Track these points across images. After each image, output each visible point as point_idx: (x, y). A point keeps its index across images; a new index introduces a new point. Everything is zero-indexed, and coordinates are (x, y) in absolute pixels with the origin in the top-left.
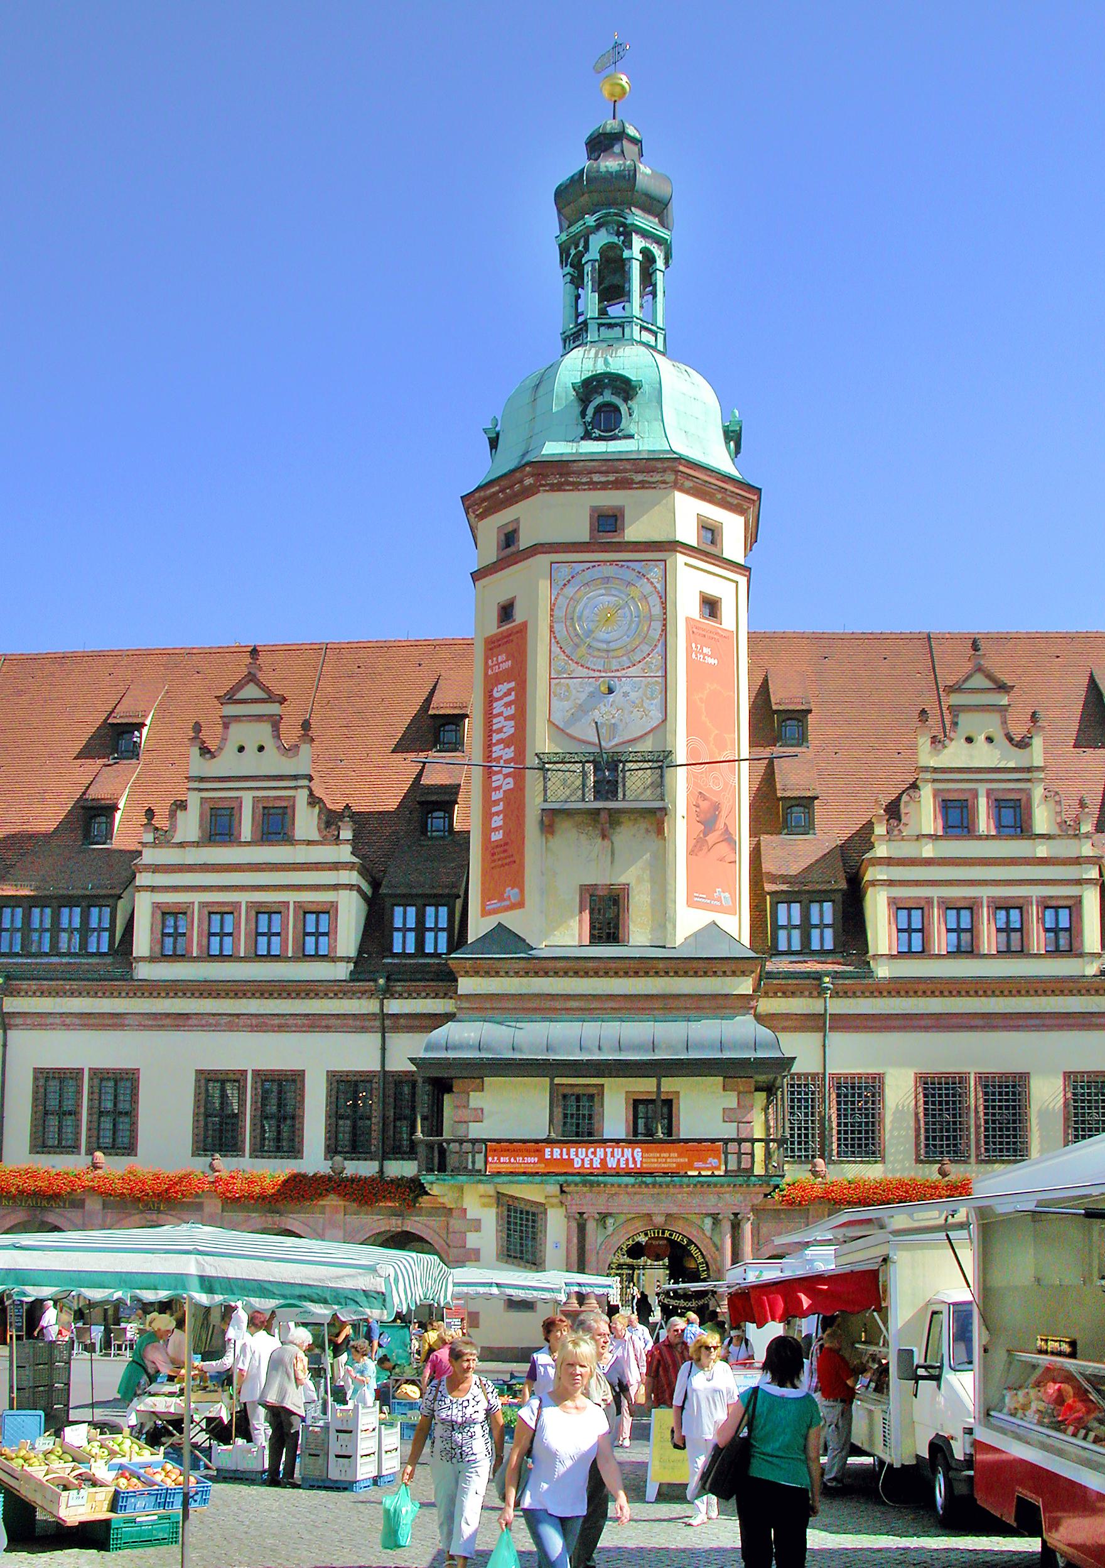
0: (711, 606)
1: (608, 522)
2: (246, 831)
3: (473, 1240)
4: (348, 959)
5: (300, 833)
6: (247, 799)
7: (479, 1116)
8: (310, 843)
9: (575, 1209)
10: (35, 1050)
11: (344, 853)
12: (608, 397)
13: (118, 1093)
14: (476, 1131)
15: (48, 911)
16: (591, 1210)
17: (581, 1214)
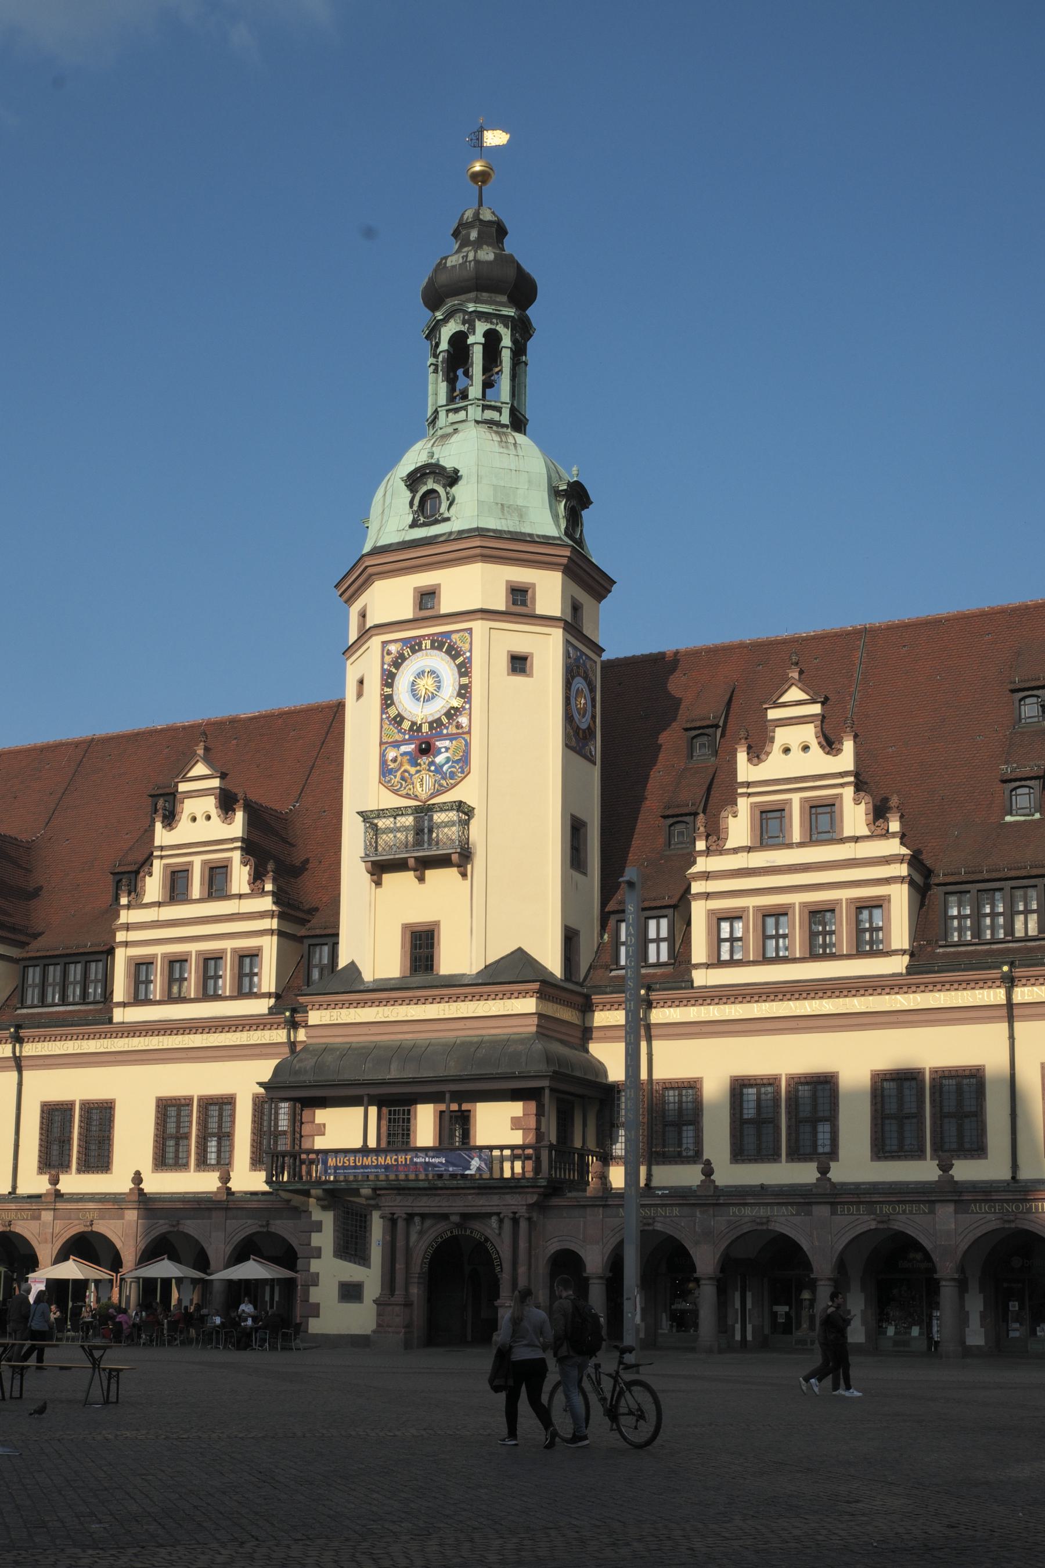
0: (519, 663)
1: (427, 597)
2: (196, 891)
3: (316, 1240)
4: (269, 995)
5: (235, 890)
6: (197, 861)
7: (321, 1130)
8: (240, 896)
9: (387, 1211)
10: (50, 1086)
11: (266, 903)
12: (430, 484)
13: (100, 1117)
14: (320, 1143)
15: (79, 966)
16: (400, 1212)
17: (393, 1214)
